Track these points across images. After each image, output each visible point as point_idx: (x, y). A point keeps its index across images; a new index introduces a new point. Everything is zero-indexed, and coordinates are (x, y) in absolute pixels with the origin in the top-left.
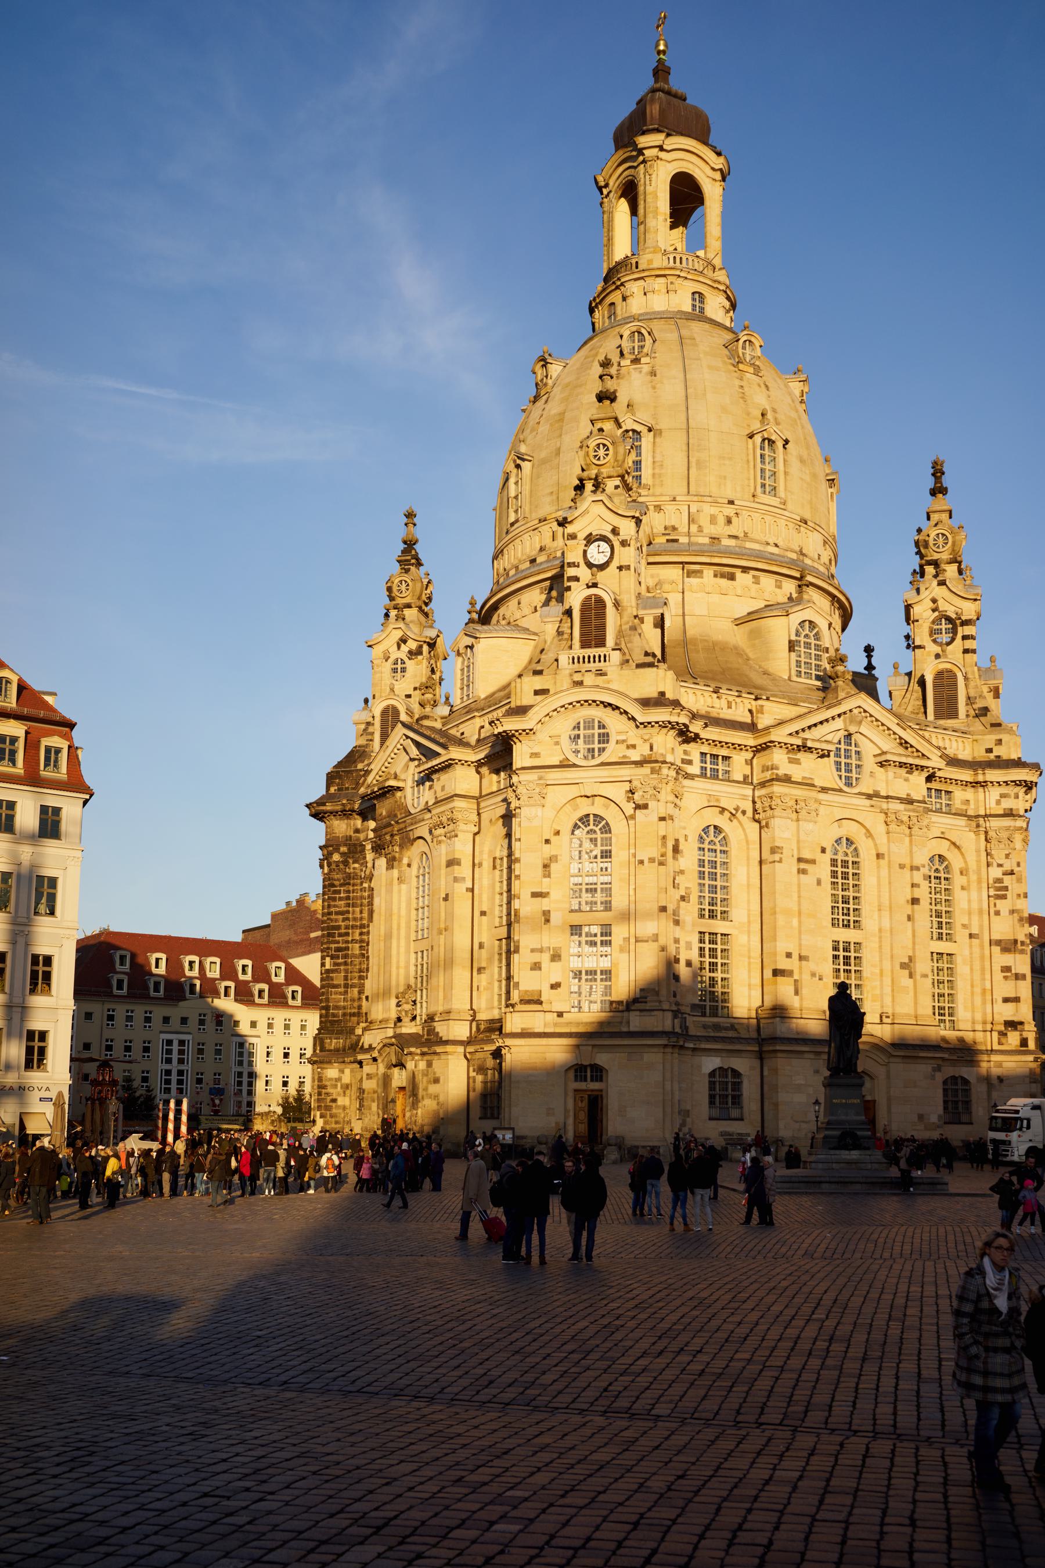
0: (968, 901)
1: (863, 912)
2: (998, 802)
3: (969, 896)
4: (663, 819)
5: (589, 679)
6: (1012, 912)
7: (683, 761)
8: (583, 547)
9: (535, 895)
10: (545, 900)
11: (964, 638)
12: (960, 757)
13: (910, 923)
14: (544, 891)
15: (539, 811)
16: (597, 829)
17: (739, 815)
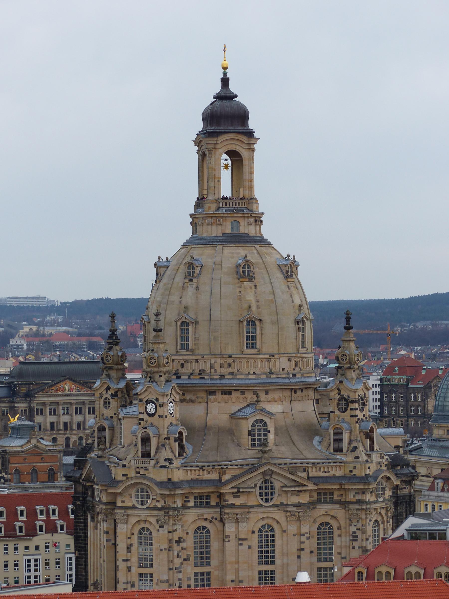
0: (339, 542)
1: (275, 557)
2: (354, 496)
3: (341, 539)
4: (169, 532)
5: (142, 472)
6: (359, 548)
7: (185, 501)
8: (145, 405)
9: (124, 560)
10: (129, 562)
11: (352, 409)
12: (337, 475)
13: (299, 559)
14: (129, 558)
15: (125, 526)
16: (148, 533)
17: (214, 520)
